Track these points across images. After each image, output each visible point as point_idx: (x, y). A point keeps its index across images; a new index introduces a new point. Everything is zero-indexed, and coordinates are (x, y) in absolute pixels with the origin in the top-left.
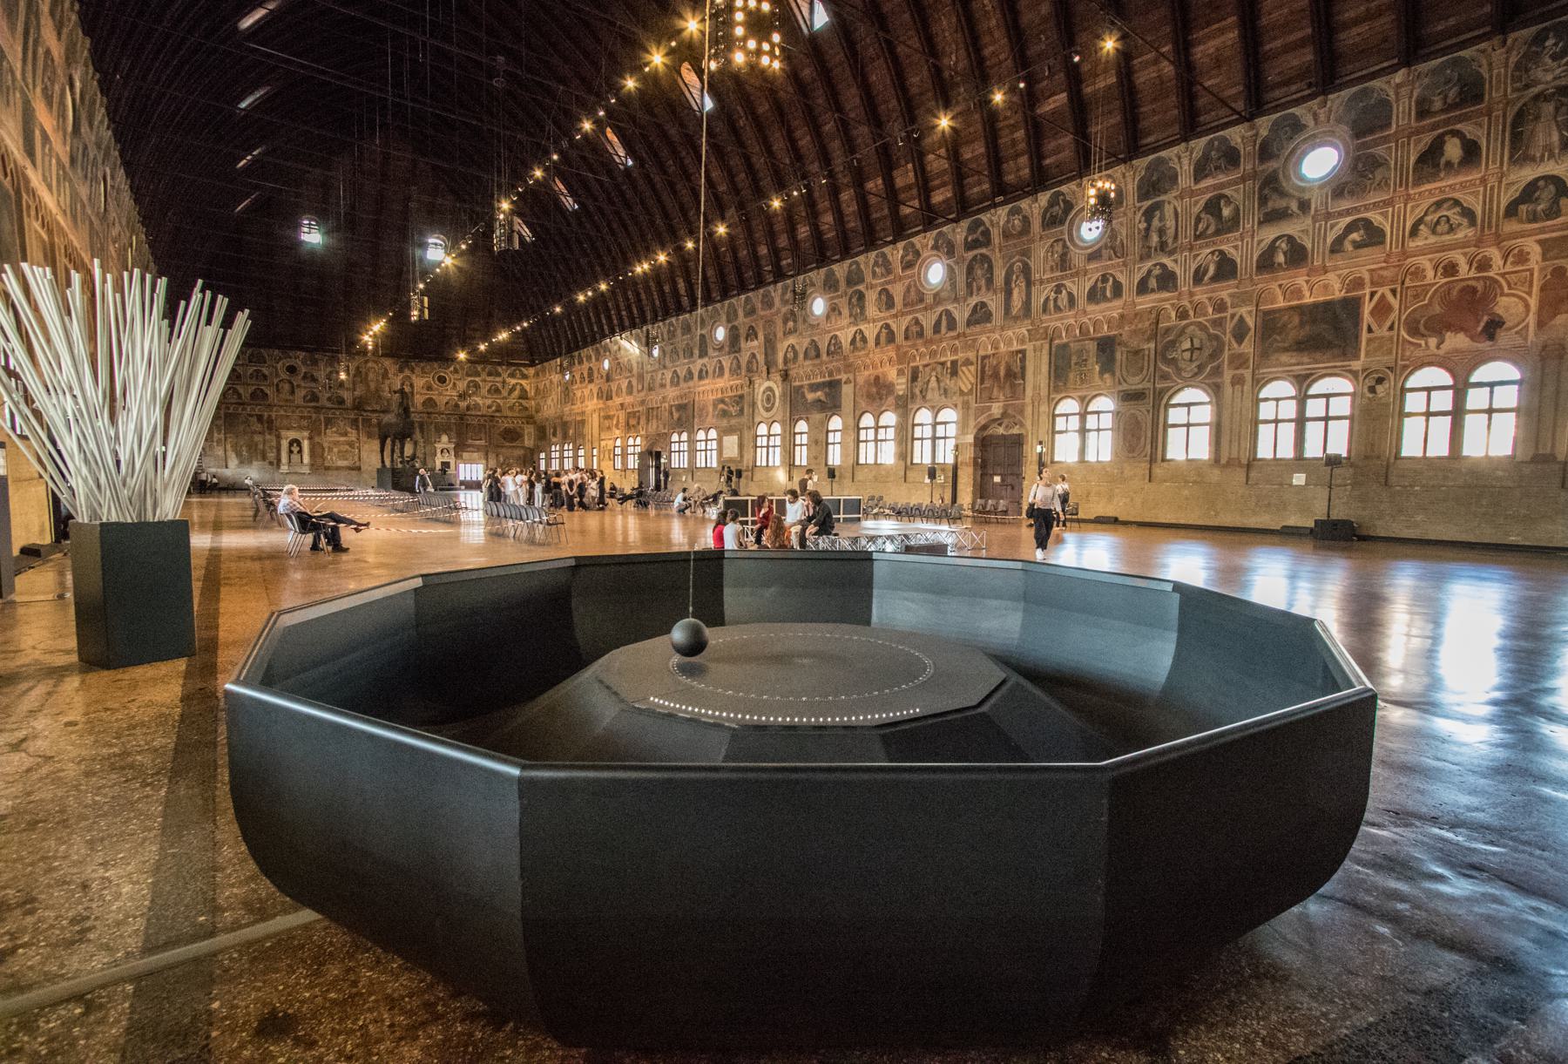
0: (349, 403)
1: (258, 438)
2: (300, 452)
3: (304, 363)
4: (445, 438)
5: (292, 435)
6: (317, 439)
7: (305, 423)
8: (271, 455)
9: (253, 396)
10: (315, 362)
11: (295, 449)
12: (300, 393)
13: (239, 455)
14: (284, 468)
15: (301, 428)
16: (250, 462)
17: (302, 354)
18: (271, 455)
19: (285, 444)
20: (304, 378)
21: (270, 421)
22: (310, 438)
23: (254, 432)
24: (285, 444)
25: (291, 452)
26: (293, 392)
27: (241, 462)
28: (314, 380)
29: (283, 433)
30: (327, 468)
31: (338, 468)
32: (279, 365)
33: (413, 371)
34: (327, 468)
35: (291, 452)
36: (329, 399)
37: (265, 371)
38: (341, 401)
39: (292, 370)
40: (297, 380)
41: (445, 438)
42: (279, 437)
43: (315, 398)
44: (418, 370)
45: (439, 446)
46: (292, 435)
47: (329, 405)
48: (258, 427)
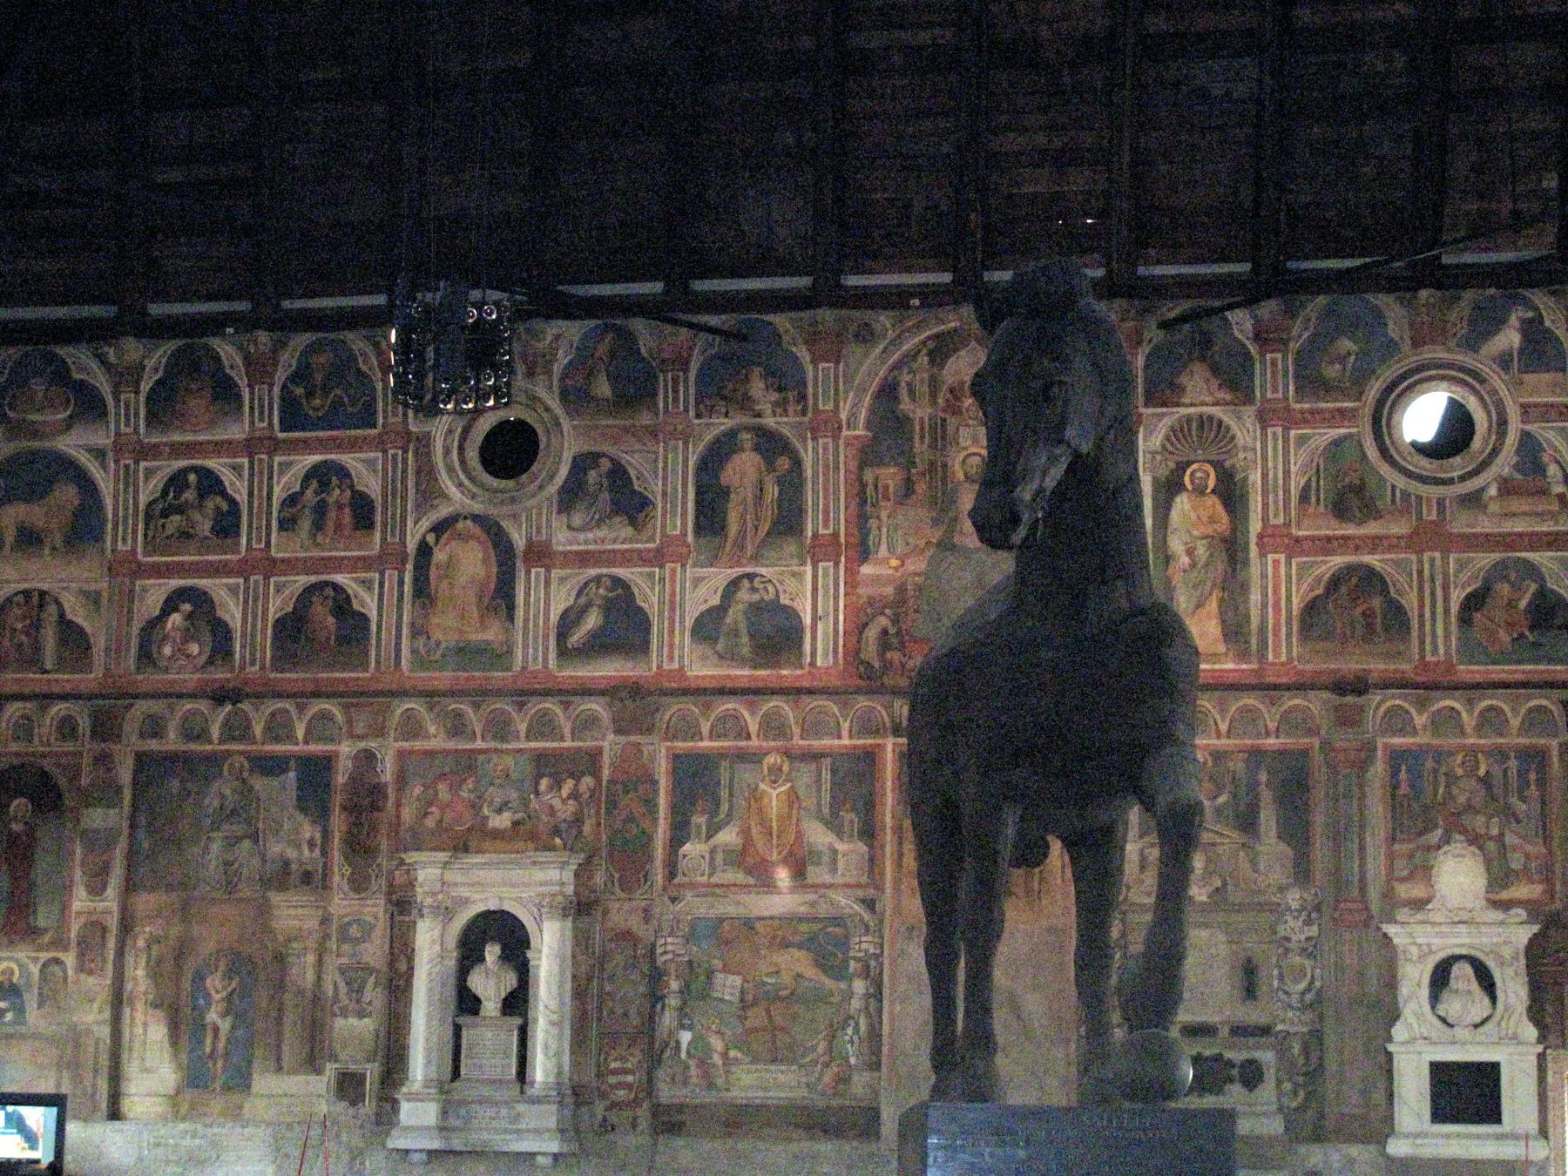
0: (823, 647)
1: (292, 913)
2: (517, 1002)
3: (576, 397)
4: (1459, 876)
5: (492, 884)
6: (622, 913)
7: (558, 801)
8: (355, 1030)
9: (292, 628)
10: (635, 389)
11: (490, 983)
12: (546, 597)
13: (183, 1025)
14: (418, 1115)
15: (528, 836)
16: (240, 1082)
17: (563, 337)
18: (355, 1030)
19: (432, 945)
20: (571, 495)
21: (367, 799)
22: (581, 907)
23: (281, 877)
24: (432, 945)
25: (468, 1003)
26: (501, 598)
27: (195, 1079)
28: (630, 503)
29: (428, 871)
30: (669, 1122)
31: (739, 1120)
32: (440, 429)
33: (1236, 379)
34: (669, 1122)
35: (468, 1003)
36: (707, 628)
37: (366, 470)
38: (777, 635)
39: (510, 452)
40: (534, 512)
41: (1459, 876)
42: (402, 905)
43: (625, 626)
44: (1274, 375)
45: (1418, 942)
46: (492, 884)
47: (702, 668)
48: (294, 837)
